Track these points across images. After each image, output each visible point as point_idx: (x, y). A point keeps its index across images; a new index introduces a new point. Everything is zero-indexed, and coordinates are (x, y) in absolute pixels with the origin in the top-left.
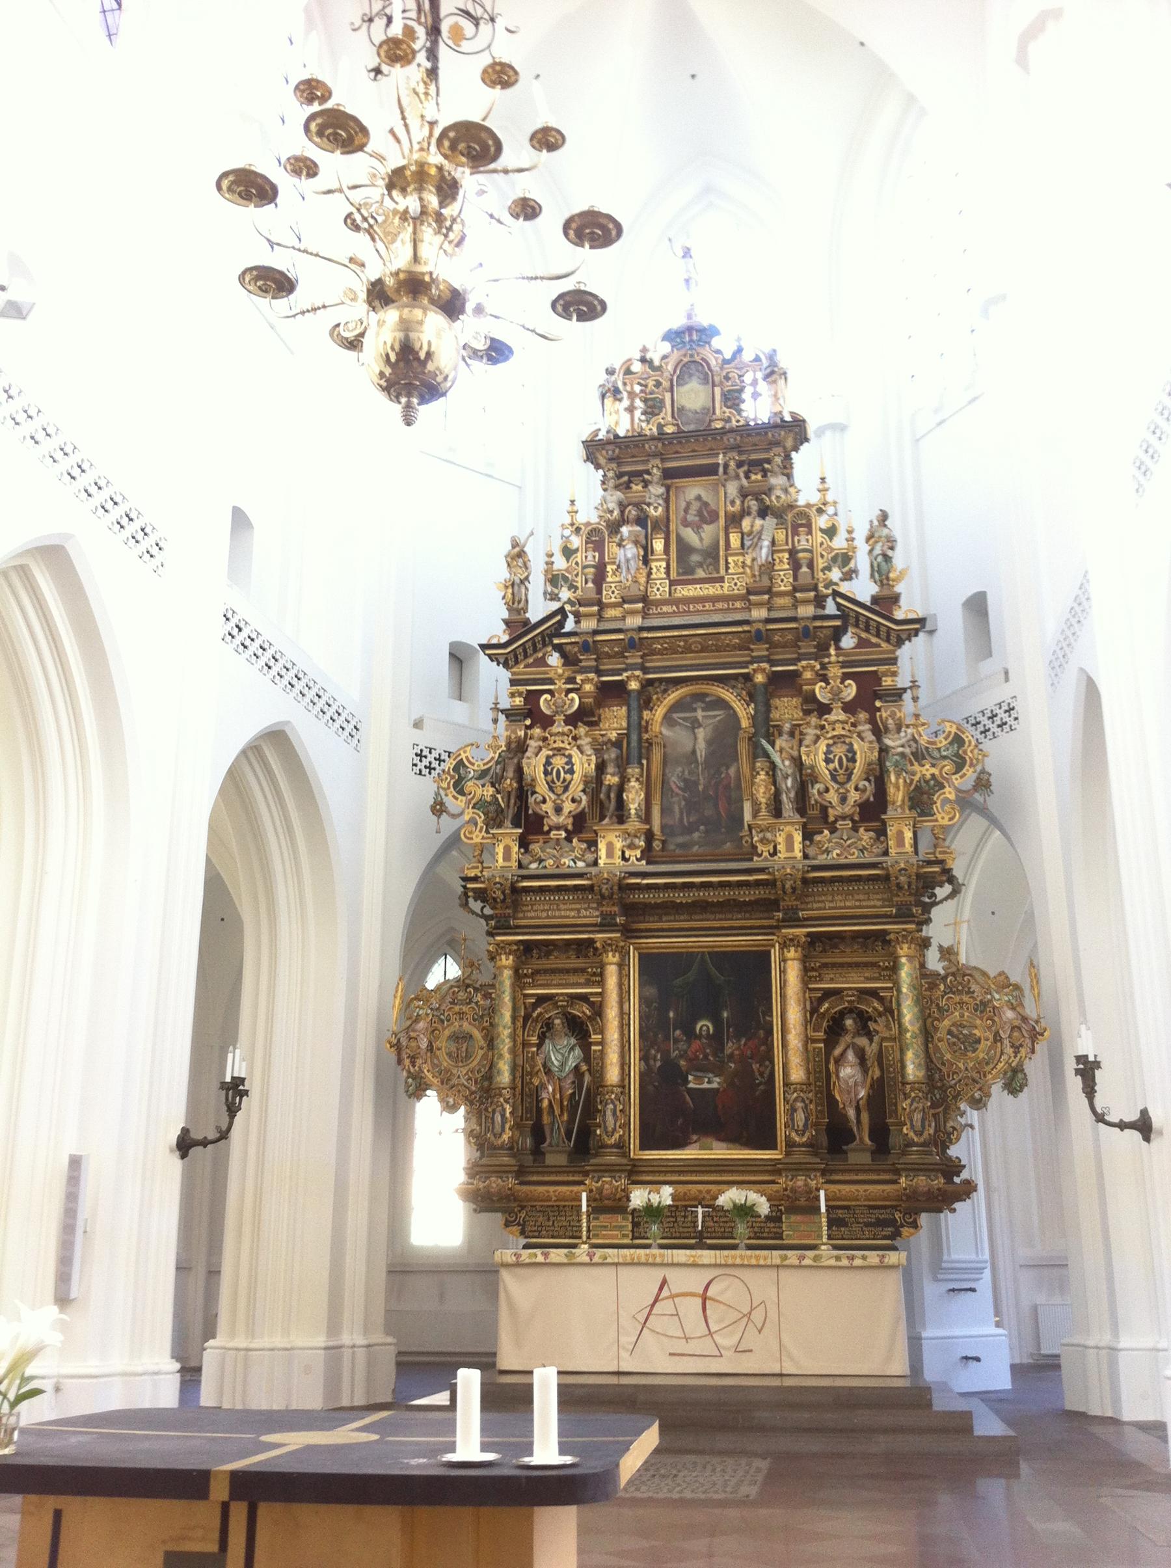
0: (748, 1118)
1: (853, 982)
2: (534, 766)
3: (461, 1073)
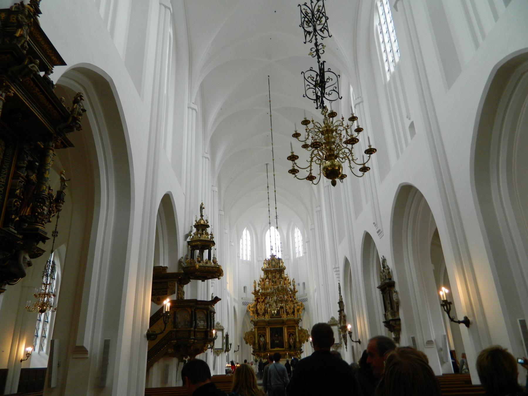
0: (281, 345)
1: (291, 331)
2: (258, 307)
3: (251, 341)
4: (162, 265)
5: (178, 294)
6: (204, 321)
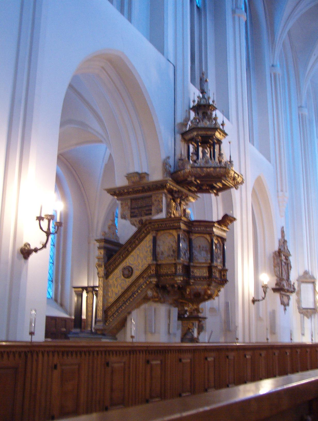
4: (137, 169)
5: (168, 212)
6: (206, 251)
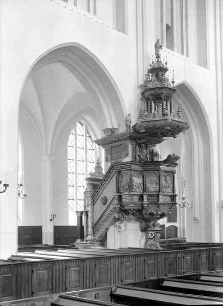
5: (134, 157)
6: (156, 183)
